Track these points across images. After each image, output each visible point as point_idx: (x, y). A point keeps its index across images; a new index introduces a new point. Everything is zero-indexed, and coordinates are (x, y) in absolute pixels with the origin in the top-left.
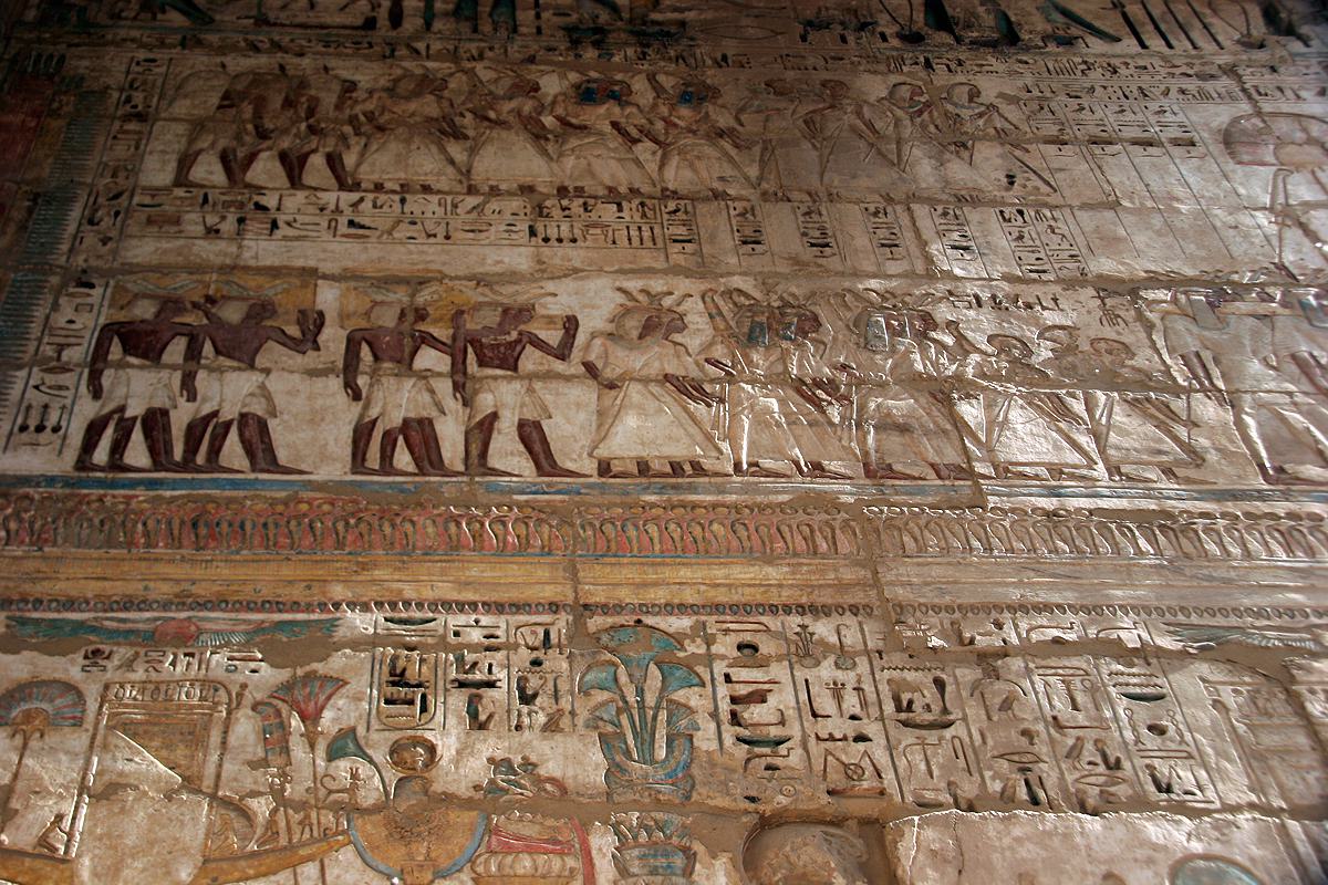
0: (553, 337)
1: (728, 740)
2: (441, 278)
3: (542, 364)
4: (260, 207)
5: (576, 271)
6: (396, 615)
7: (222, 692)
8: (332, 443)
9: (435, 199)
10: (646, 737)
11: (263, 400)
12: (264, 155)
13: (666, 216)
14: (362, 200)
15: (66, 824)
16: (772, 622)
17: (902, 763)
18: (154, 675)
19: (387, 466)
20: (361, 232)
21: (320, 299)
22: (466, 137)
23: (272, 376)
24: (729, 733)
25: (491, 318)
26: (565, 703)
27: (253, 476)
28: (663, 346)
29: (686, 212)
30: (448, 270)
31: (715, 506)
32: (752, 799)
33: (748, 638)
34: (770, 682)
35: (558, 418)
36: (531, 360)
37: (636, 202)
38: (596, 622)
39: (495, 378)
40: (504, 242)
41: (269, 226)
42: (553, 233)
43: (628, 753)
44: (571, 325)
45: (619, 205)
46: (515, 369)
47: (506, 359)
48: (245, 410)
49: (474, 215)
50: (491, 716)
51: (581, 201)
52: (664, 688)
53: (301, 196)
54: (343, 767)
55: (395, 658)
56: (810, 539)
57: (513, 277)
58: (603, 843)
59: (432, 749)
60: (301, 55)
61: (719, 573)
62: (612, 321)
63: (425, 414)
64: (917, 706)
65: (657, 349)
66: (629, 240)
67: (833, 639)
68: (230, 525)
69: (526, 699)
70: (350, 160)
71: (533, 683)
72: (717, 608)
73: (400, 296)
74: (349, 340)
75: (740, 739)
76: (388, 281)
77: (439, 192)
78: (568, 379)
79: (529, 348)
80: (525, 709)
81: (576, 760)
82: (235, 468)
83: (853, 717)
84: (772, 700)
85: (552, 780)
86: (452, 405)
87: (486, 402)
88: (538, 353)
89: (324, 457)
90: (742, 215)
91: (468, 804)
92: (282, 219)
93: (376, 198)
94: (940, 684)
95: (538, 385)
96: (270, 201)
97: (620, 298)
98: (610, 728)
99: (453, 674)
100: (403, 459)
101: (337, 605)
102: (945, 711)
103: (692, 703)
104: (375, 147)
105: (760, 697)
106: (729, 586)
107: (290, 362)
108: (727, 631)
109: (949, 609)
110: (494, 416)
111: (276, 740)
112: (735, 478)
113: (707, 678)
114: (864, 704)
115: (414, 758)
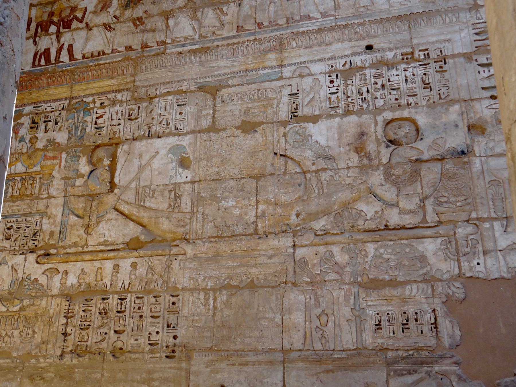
0: (79, 15)
1: (93, 128)
10: (76, 129)
16: (109, 96)
17: (125, 130)
19: (39, 65)
24: (94, 126)
25: (68, 12)
26: (63, 124)
28: (105, 13)
31: (105, 64)
32: (94, 142)
33: (103, 101)
35: (77, 43)
36: (75, 24)
38: (74, 101)
39: (65, 32)
43: (72, 135)
47: (68, 25)
54: (21, 143)
56: (123, 70)
58: (64, 155)
61: (101, 84)
62: (95, 7)
64: (133, 115)
67: (120, 99)
72: (99, 94)
73: (48, 9)
79: (75, 20)
80: (55, 126)
81: (61, 137)
83: (119, 119)
84: (104, 117)
85: (58, 143)
86: (55, 43)
87: (62, 40)
89: (27, 64)
94: (139, 107)
99: (43, 120)
100: (43, 62)
102: (138, 115)
103: (88, 120)
105: (101, 117)
106: (103, 87)
109: (147, 86)
110: (63, 44)
114: (122, 116)
115: (34, 140)
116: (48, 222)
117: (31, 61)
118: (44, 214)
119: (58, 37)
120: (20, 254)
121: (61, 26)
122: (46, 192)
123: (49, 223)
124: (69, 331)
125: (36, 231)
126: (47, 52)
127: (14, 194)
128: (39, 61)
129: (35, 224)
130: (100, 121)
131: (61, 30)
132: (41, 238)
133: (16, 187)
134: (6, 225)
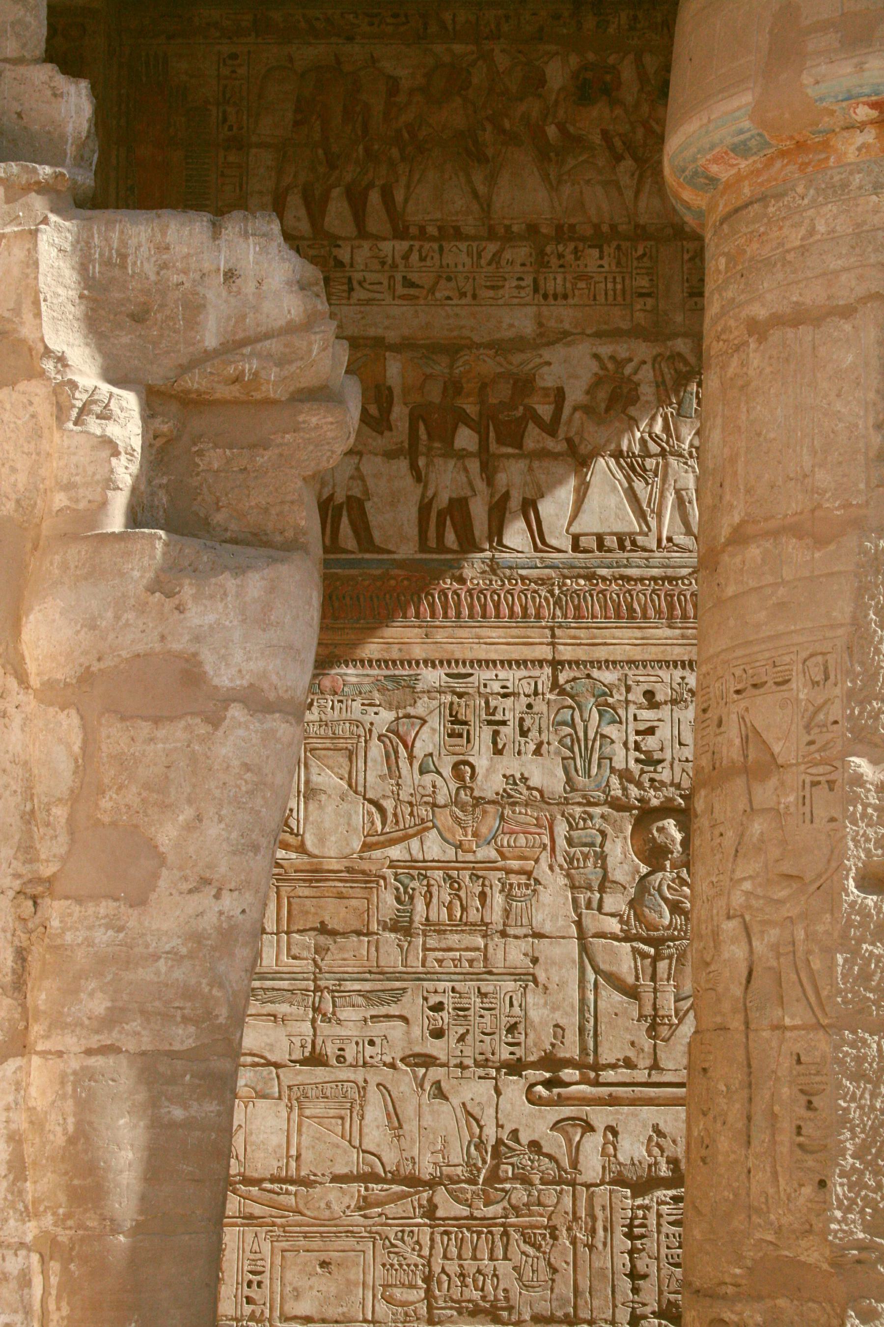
0: (545, 411)
2: (472, 345)
3: (538, 441)
4: (340, 264)
5: (566, 334)
6: (450, 671)
7: (361, 729)
8: (406, 523)
9: (463, 246)
11: (359, 482)
12: (336, 193)
13: (635, 263)
14: (411, 248)
15: (295, 814)
16: (664, 674)
18: (323, 716)
19: (442, 548)
20: (412, 291)
21: (388, 374)
22: (487, 161)
23: (364, 459)
27: (360, 556)
29: (651, 257)
30: (477, 339)
34: (659, 720)
36: (533, 437)
37: (614, 244)
39: (508, 456)
40: (516, 301)
41: (345, 287)
42: (550, 287)
44: (560, 395)
45: (600, 247)
46: (520, 446)
47: (513, 436)
48: (350, 493)
49: (494, 265)
50: (505, 745)
51: (572, 246)
52: (599, 726)
53: (366, 245)
54: (428, 779)
55: (452, 704)
57: (519, 344)
59: (473, 767)
60: (350, 39)
62: (588, 392)
63: (462, 494)
65: (617, 424)
66: (606, 294)
68: (351, 598)
69: (524, 733)
70: (399, 195)
71: (528, 723)
73: (440, 367)
74: (411, 414)
75: (637, 761)
76: (434, 349)
77: (467, 238)
78: (555, 456)
79: (531, 425)
80: (523, 740)
81: (547, 775)
82: (350, 548)
84: (658, 732)
86: (480, 485)
87: (502, 479)
88: (537, 430)
90: (692, 259)
91: (493, 802)
92: (357, 276)
93: (421, 247)
95: (536, 464)
96: (344, 254)
97: (594, 366)
98: (568, 753)
99: (484, 717)
100: (450, 538)
101: (418, 663)
104: (417, 177)
105: (651, 731)
107: (374, 444)
108: (638, 682)
110: (506, 496)
111: (391, 758)
112: (657, 554)
113: (624, 719)
116: (542, 1001)
117: (412, 531)
118: (527, 978)
119: (489, 472)
120: (480, 1078)
121: (492, 435)
122: (525, 921)
123: (546, 1003)
124: (641, 1267)
125: (512, 1021)
126: (459, 509)
127: (433, 917)
128: (440, 537)
129: (507, 1002)
130: (650, 743)
131: (493, 447)
132: (530, 1041)
133: (435, 900)
134: (425, 999)
